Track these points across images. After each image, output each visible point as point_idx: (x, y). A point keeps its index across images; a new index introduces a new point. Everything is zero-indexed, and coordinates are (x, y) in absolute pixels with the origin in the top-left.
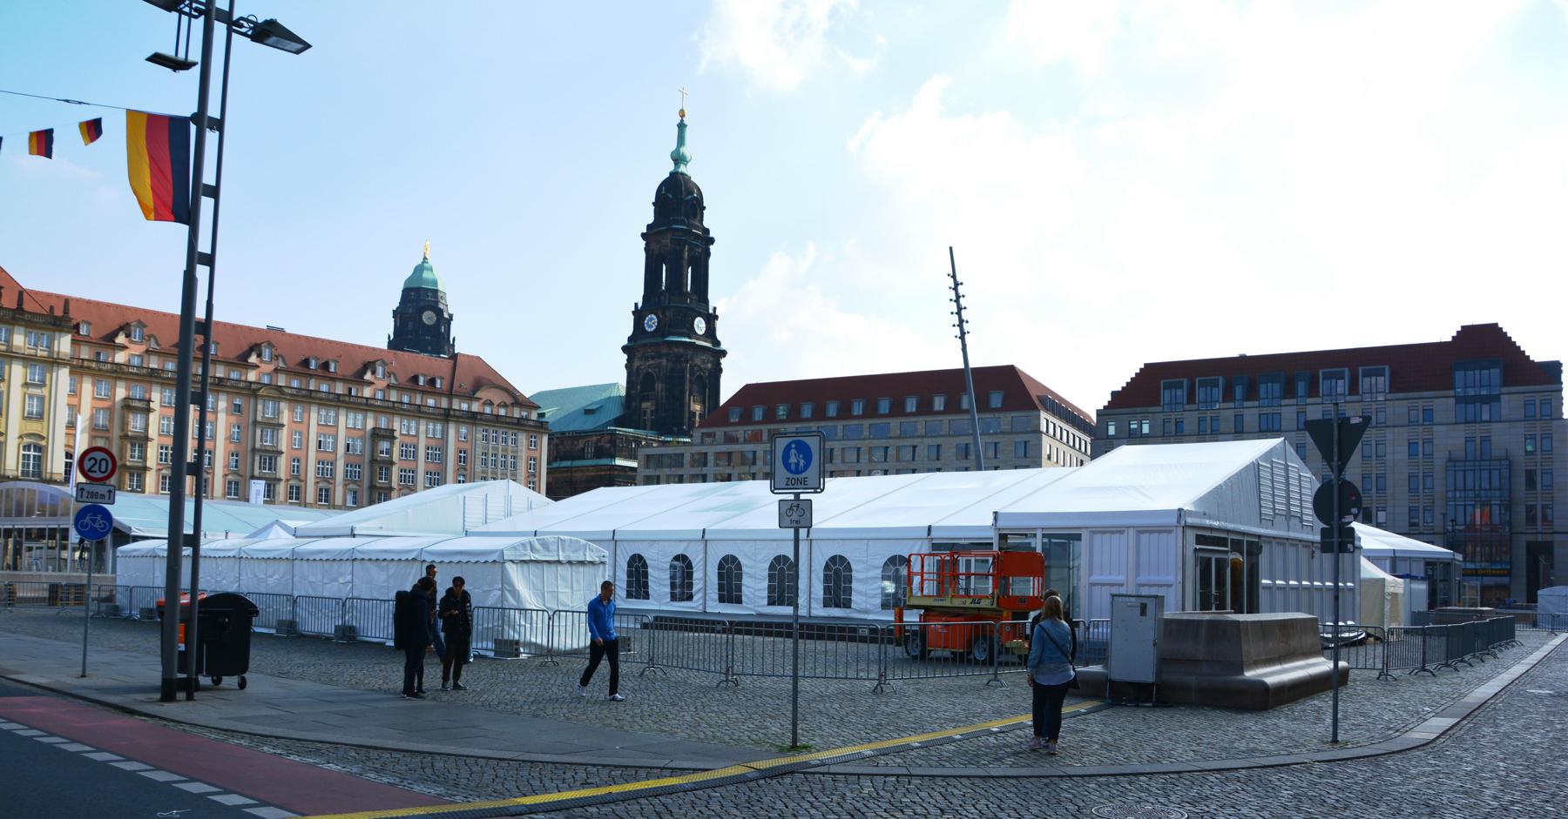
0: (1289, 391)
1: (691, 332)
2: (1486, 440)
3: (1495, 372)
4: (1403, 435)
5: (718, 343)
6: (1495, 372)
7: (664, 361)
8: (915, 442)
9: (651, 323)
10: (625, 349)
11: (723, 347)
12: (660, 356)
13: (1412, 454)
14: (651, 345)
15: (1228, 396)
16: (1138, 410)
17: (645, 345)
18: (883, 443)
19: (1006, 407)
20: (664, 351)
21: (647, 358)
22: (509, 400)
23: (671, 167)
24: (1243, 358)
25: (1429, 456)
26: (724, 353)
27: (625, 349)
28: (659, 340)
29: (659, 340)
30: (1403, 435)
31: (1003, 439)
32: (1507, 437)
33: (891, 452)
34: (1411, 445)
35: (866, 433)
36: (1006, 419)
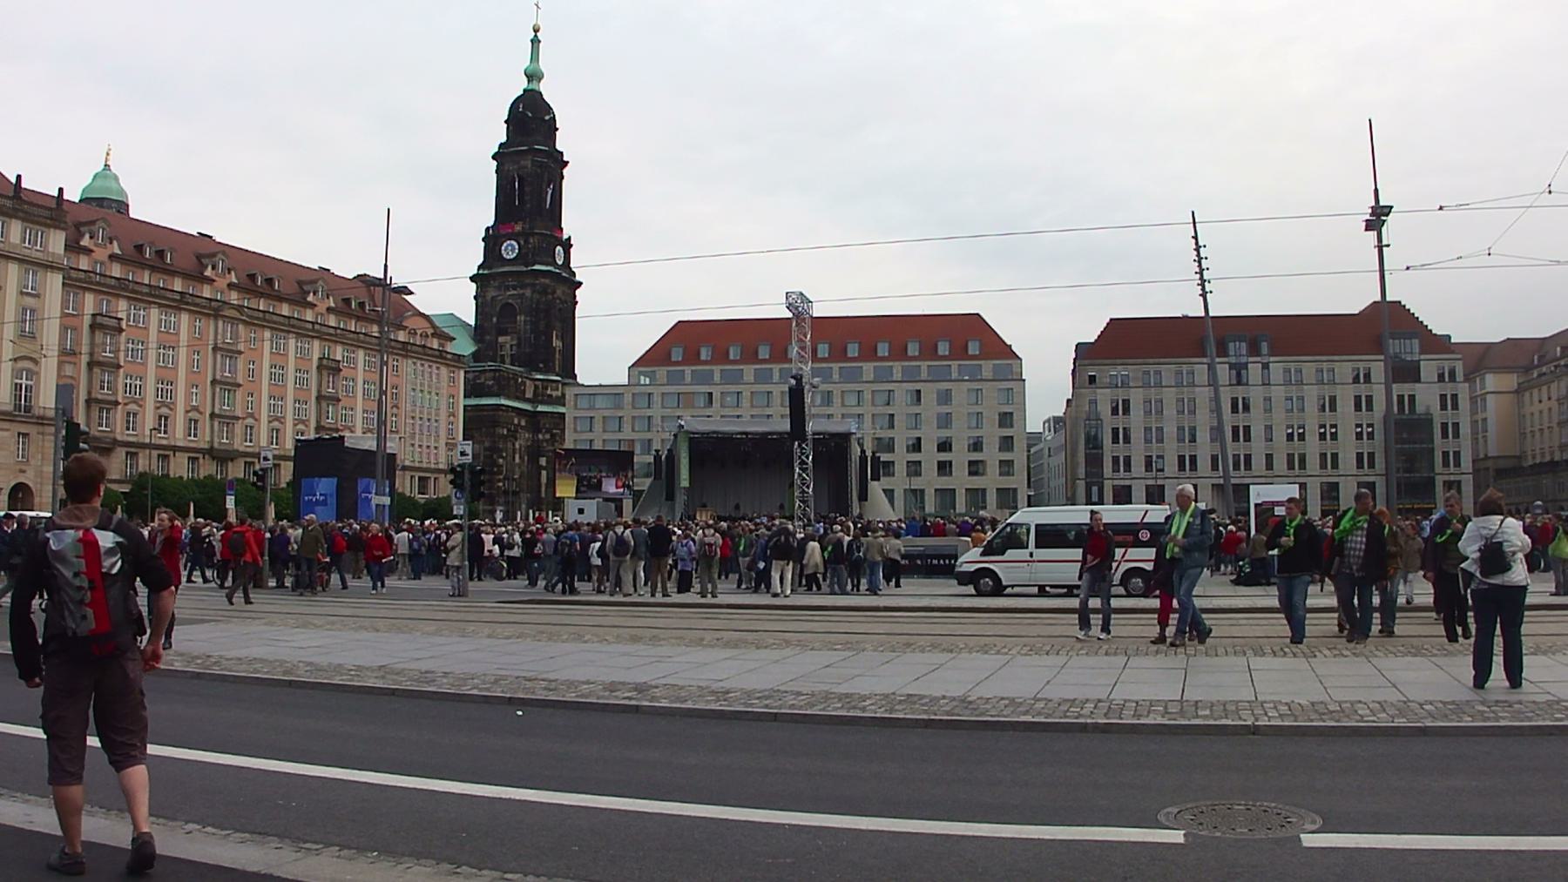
0: (1254, 350)
1: (554, 264)
2: (1412, 398)
3: (1416, 342)
5: (574, 274)
6: (1416, 342)
7: (528, 292)
8: (918, 386)
9: (510, 250)
11: (578, 278)
12: (523, 287)
13: (1358, 407)
18: (857, 387)
19: (984, 355)
22: (430, 331)
23: (523, 84)
24: (1185, 317)
25: (1370, 408)
31: (984, 386)
32: (1426, 395)
33: (867, 396)
34: (1358, 399)
35: (836, 377)
36: (987, 368)
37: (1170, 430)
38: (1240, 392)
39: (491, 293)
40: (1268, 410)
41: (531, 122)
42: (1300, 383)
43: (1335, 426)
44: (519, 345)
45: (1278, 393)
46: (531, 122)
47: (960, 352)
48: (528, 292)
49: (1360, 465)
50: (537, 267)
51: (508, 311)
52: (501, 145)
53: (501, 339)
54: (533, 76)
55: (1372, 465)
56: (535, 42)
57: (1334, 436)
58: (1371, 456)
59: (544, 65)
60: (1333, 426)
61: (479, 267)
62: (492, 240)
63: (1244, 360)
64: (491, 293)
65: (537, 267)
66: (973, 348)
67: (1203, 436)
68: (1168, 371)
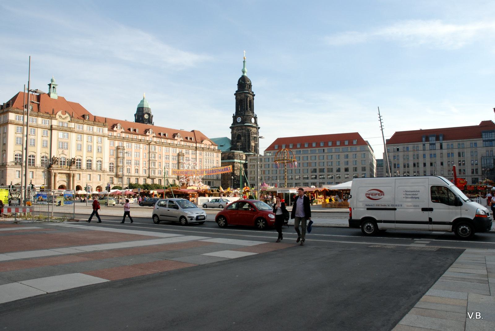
4: (469, 150)
9: (239, 120)
10: (231, 128)
14: (240, 126)
15: (422, 141)
16: (396, 144)
17: (238, 126)
19: (358, 144)
20: (244, 128)
21: (238, 130)
26: (259, 128)
27: (231, 128)
28: (242, 125)
29: (242, 125)
30: (469, 150)
36: (358, 148)
37: (411, 164)
38: (433, 152)
39: (235, 131)
40: (441, 157)
41: (244, 85)
42: (452, 148)
43: (464, 161)
44: (242, 145)
45: (445, 152)
46: (244, 85)
47: (351, 143)
48: (244, 131)
49: (473, 173)
50: (246, 124)
51: (239, 137)
52: (237, 92)
53: (238, 144)
54: (244, 72)
55: (477, 173)
56: (244, 62)
57: (464, 164)
58: (477, 169)
59: (246, 70)
60: (463, 161)
61: (232, 125)
62: (235, 118)
63: (434, 142)
64: (235, 131)
65: (246, 124)
66: (355, 142)
67: (421, 165)
68: (411, 146)
